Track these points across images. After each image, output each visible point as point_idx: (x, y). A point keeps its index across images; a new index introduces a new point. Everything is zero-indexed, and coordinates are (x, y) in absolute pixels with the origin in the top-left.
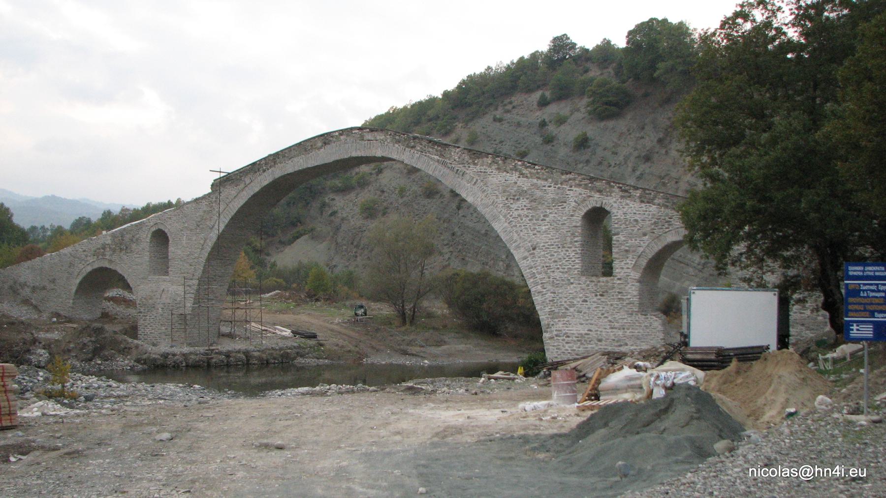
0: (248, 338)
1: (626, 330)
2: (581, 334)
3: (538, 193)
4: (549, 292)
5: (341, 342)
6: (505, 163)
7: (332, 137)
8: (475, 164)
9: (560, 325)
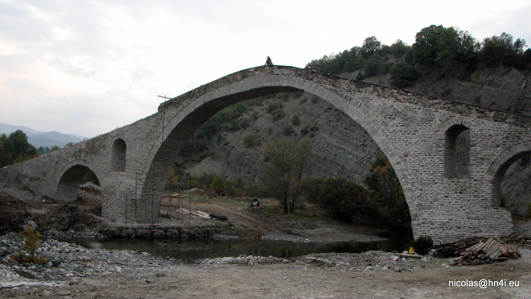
0: (180, 218)
1: (480, 220)
2: (444, 222)
3: (410, 114)
4: (417, 189)
5: (245, 224)
6: (383, 91)
7: (249, 72)
8: (359, 92)
9: (426, 214)
